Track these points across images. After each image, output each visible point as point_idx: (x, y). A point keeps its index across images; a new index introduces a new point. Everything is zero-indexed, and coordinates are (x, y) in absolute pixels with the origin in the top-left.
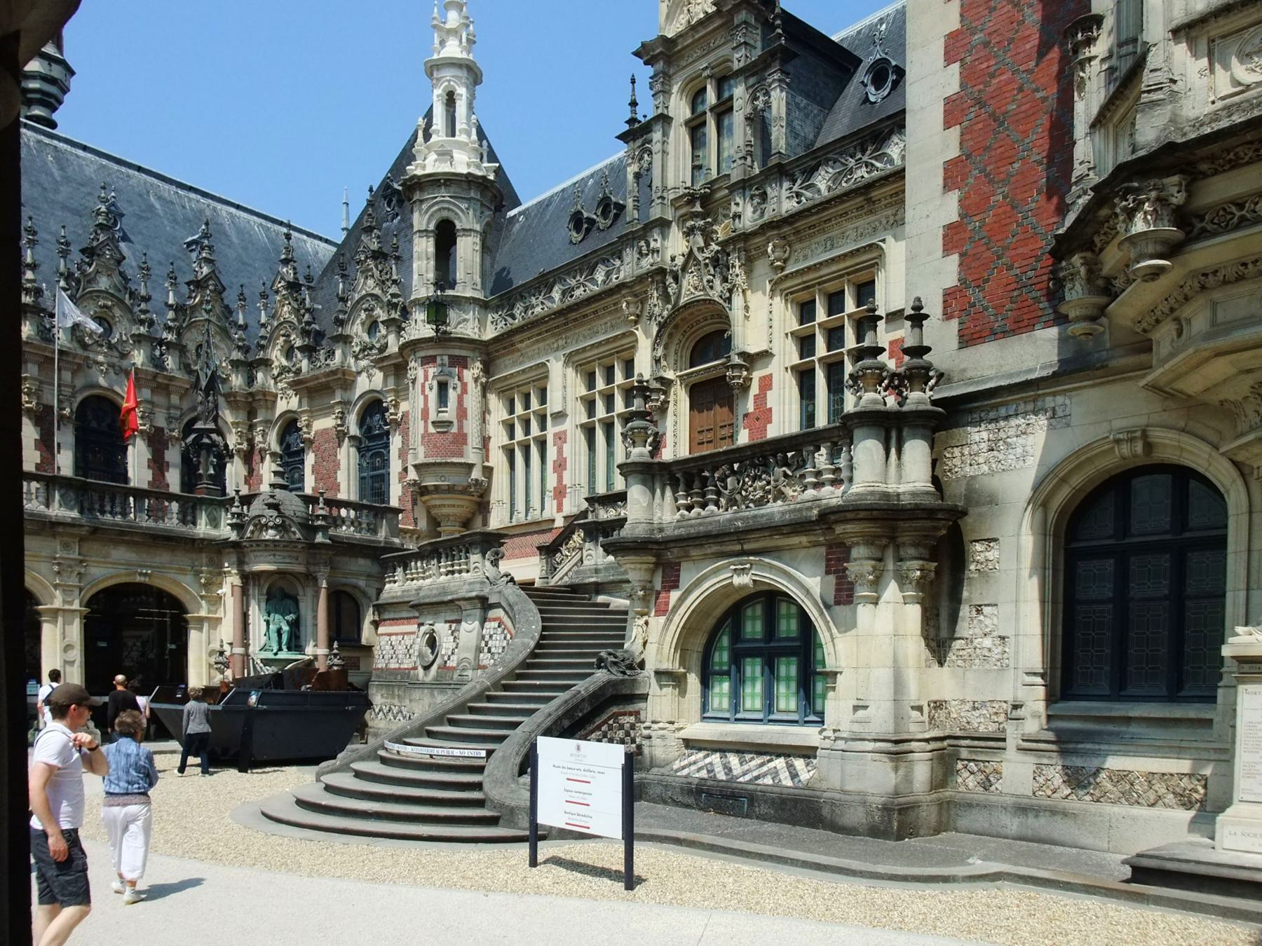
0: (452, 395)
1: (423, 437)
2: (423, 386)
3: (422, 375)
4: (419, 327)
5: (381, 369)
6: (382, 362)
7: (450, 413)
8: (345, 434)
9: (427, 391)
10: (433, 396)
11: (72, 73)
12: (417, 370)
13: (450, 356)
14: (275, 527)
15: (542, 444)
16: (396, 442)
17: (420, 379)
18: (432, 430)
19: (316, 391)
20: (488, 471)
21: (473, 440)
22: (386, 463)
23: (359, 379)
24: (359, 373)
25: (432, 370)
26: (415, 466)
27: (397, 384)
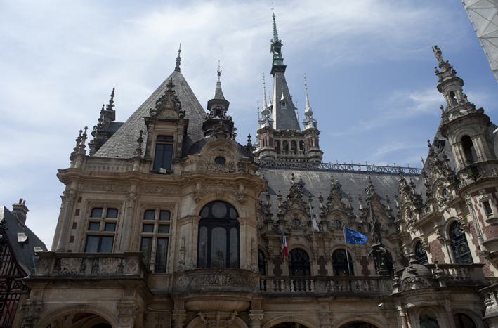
1: (483, 229)
5: (452, 207)
6: (452, 204)
8: (443, 240)
11: (323, 153)
13: (485, 189)
14: (416, 282)
16: (469, 237)
17: (474, 204)
18: (487, 225)
19: (425, 227)
22: (468, 248)
23: (444, 214)
24: (443, 212)
25: (478, 198)
26: (483, 244)
27: (462, 211)
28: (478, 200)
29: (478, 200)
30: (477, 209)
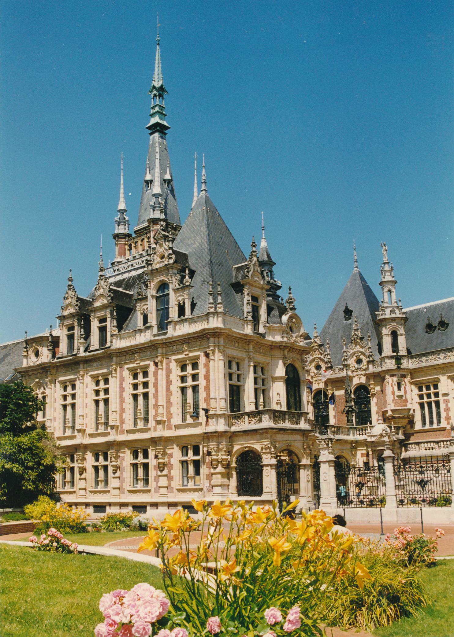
0: (402, 387)
1: (393, 400)
2: (392, 384)
3: (391, 382)
4: (391, 364)
7: (402, 393)
9: (394, 386)
10: (396, 388)
12: (388, 379)
15: (437, 403)
18: (396, 398)
20: (414, 410)
21: (409, 400)
24: (354, 377)
25: (395, 379)
26: (391, 410)
28: (395, 381)
29: (395, 381)
30: (392, 386)
